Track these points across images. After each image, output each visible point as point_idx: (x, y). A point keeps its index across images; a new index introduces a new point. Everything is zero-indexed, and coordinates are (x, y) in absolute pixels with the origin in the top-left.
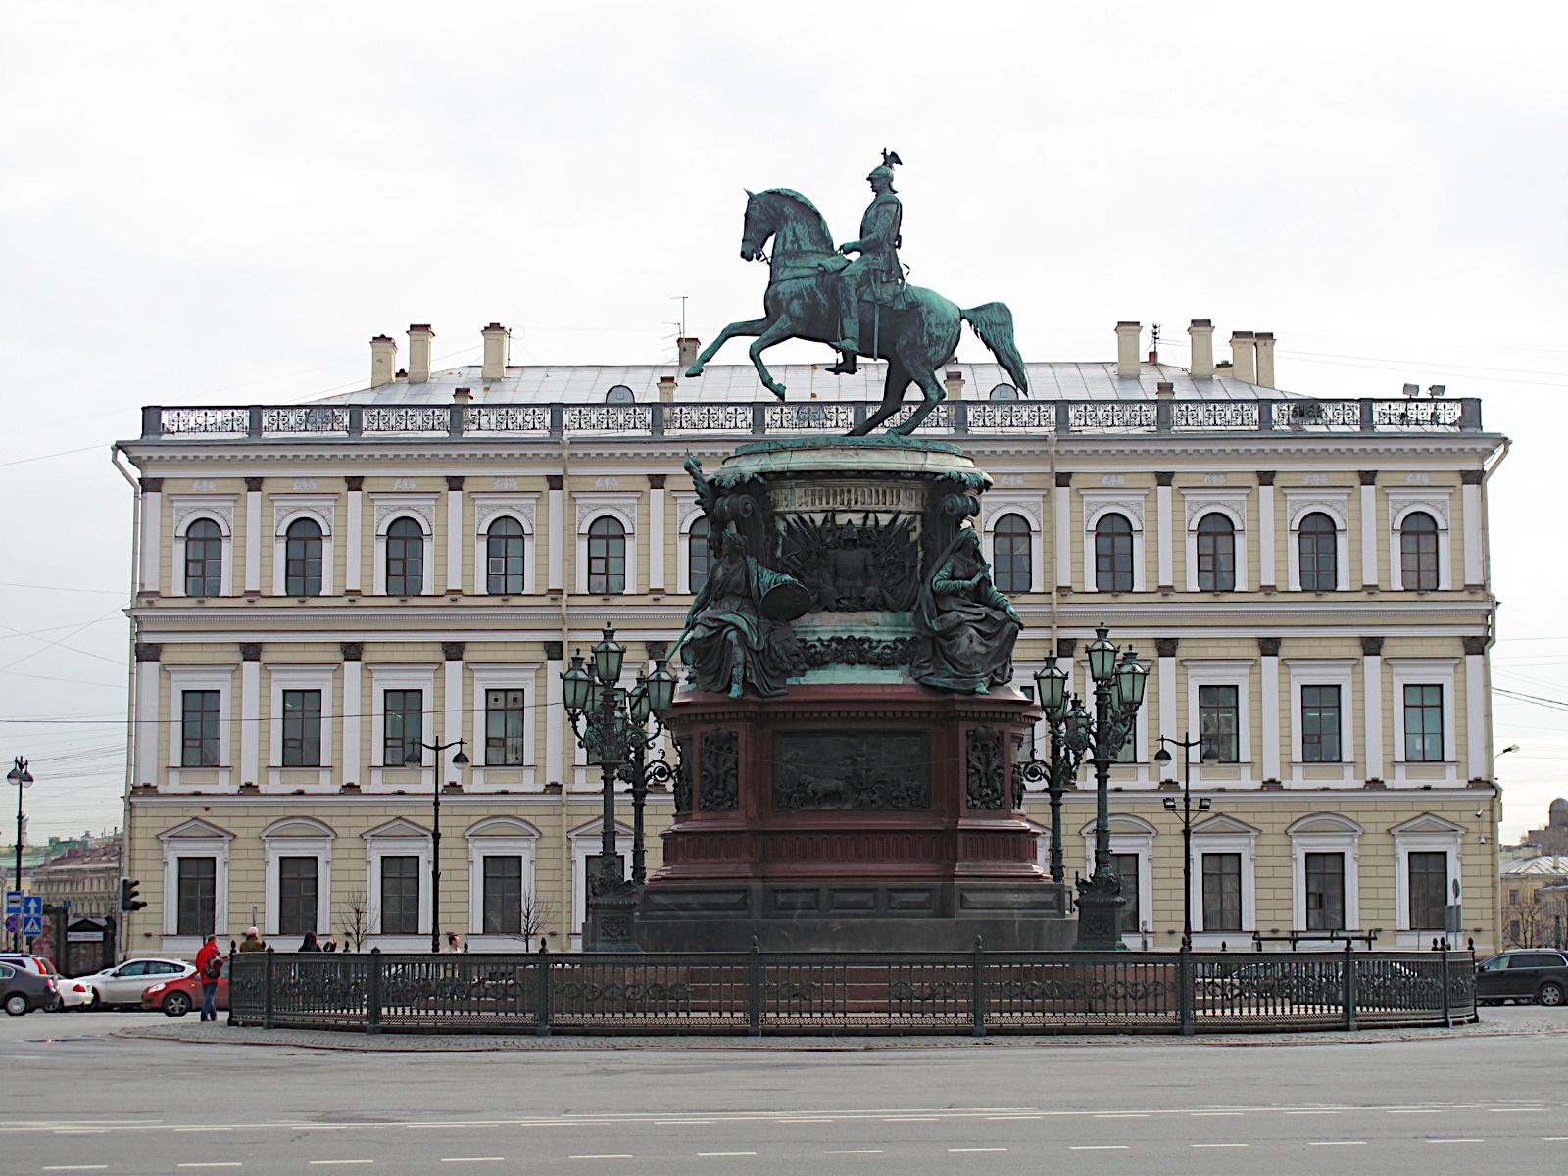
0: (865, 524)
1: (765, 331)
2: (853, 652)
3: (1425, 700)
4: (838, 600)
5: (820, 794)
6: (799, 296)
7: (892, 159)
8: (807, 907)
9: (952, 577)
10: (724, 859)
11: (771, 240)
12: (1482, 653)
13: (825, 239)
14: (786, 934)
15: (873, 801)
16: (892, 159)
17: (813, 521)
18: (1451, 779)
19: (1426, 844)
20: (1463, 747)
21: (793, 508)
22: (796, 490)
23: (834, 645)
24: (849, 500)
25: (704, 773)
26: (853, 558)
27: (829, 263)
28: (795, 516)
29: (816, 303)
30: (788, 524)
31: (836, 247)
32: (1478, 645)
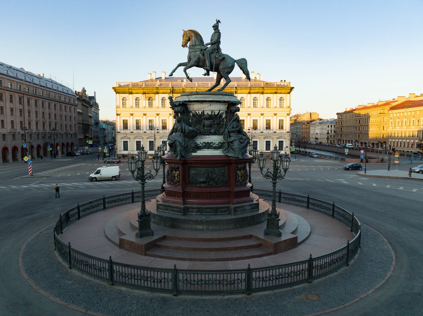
0: (212, 114)
1: (187, 66)
2: (208, 146)
4: (205, 133)
7: (218, 22)
9: (233, 128)
10: (176, 198)
13: (202, 41)
14: (191, 222)
16: (218, 22)
17: (199, 113)
23: (204, 144)
25: (172, 176)
26: (207, 122)
27: (203, 48)
31: (205, 44)
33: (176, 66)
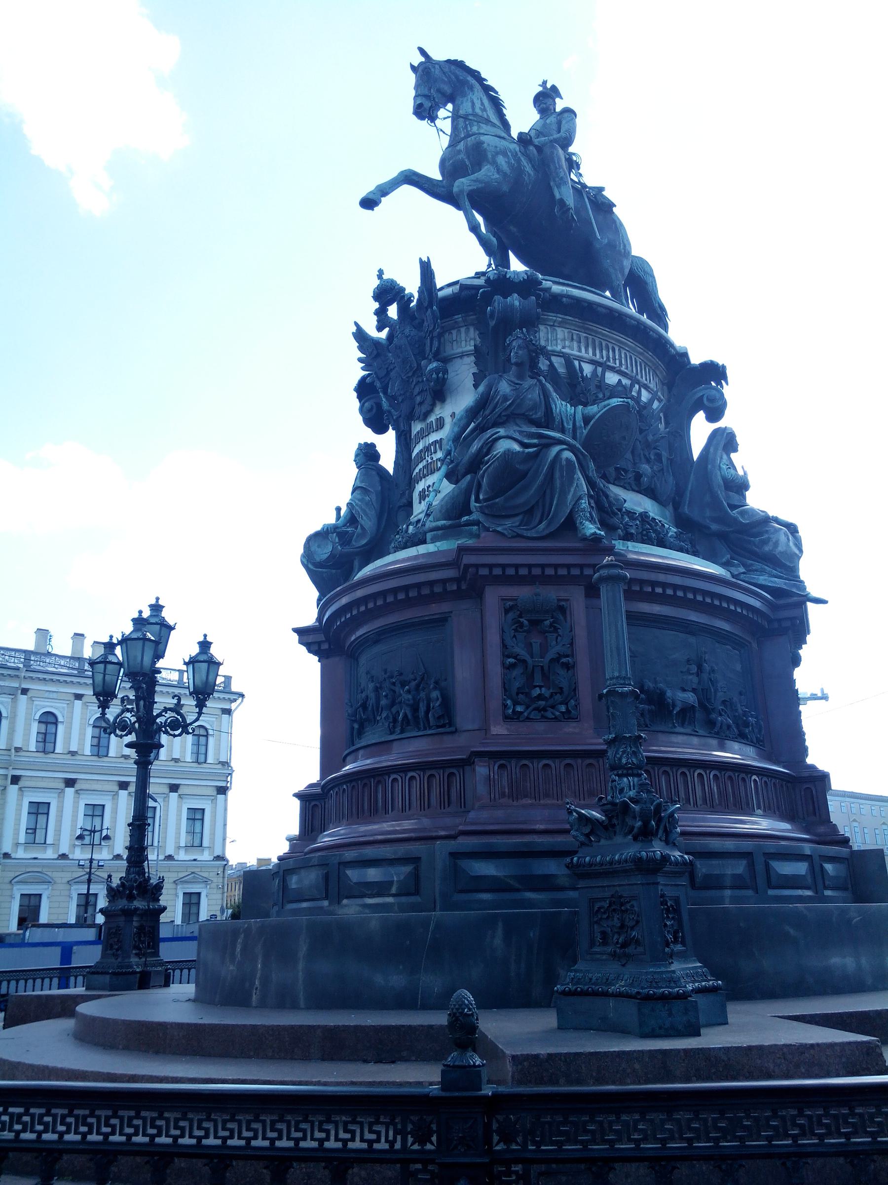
3: (196, 816)
5: (678, 709)
6: (504, 153)
8: (739, 883)
11: (450, 106)
12: (225, 794)
13: (506, 126)
14: (792, 931)
15: (729, 727)
18: (206, 856)
19: (192, 888)
20: (212, 840)
21: (559, 348)
22: (559, 330)
24: (615, 359)
25: (512, 660)
28: (562, 360)
29: (518, 171)
30: (551, 365)
32: (223, 791)
33: (392, 174)
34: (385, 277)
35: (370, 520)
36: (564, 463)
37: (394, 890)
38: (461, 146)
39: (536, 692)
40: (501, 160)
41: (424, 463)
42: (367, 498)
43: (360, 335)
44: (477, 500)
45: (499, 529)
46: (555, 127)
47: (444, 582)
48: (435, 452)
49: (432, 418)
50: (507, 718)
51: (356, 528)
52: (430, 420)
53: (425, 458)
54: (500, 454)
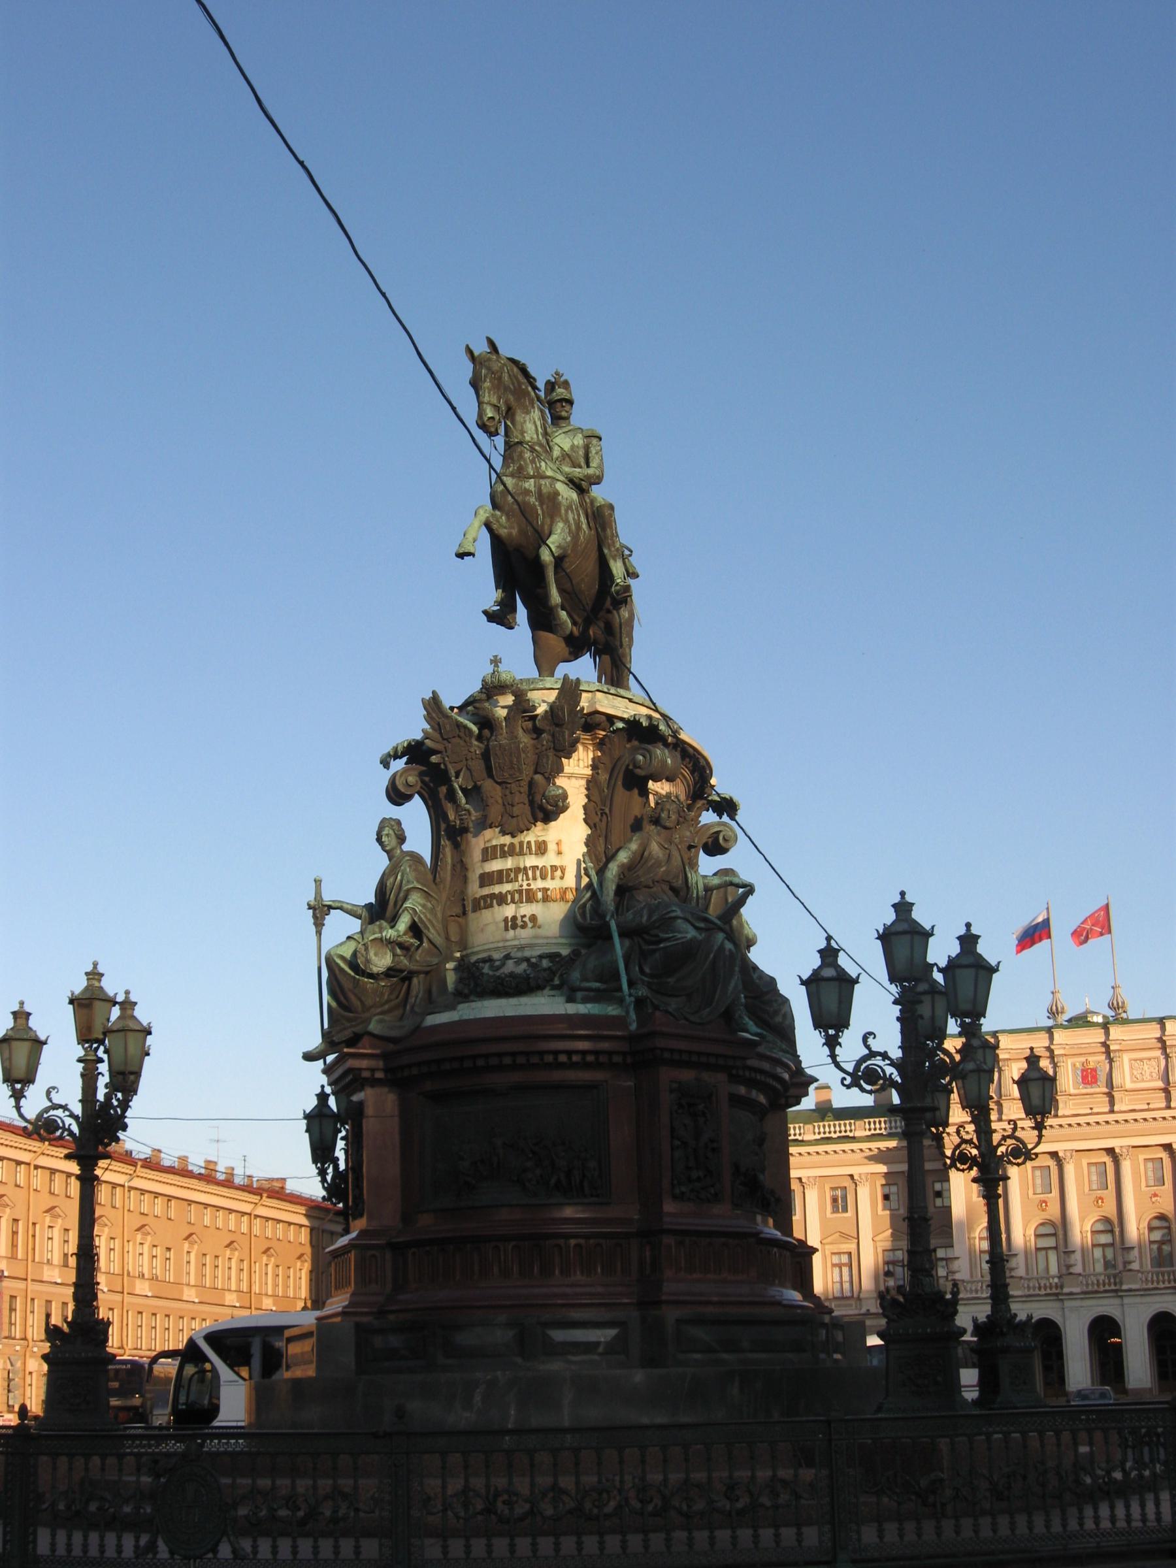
34: (502, 668)
35: (439, 935)
36: (727, 953)
37: (601, 1349)
38: (530, 484)
39: (695, 1174)
40: (570, 516)
41: (516, 886)
42: (429, 905)
43: (433, 705)
44: (642, 971)
45: (670, 1010)
46: (581, 452)
47: (610, 1053)
48: (535, 879)
49: (531, 836)
50: (675, 1197)
51: (422, 942)
52: (527, 839)
53: (518, 881)
54: (684, 940)
